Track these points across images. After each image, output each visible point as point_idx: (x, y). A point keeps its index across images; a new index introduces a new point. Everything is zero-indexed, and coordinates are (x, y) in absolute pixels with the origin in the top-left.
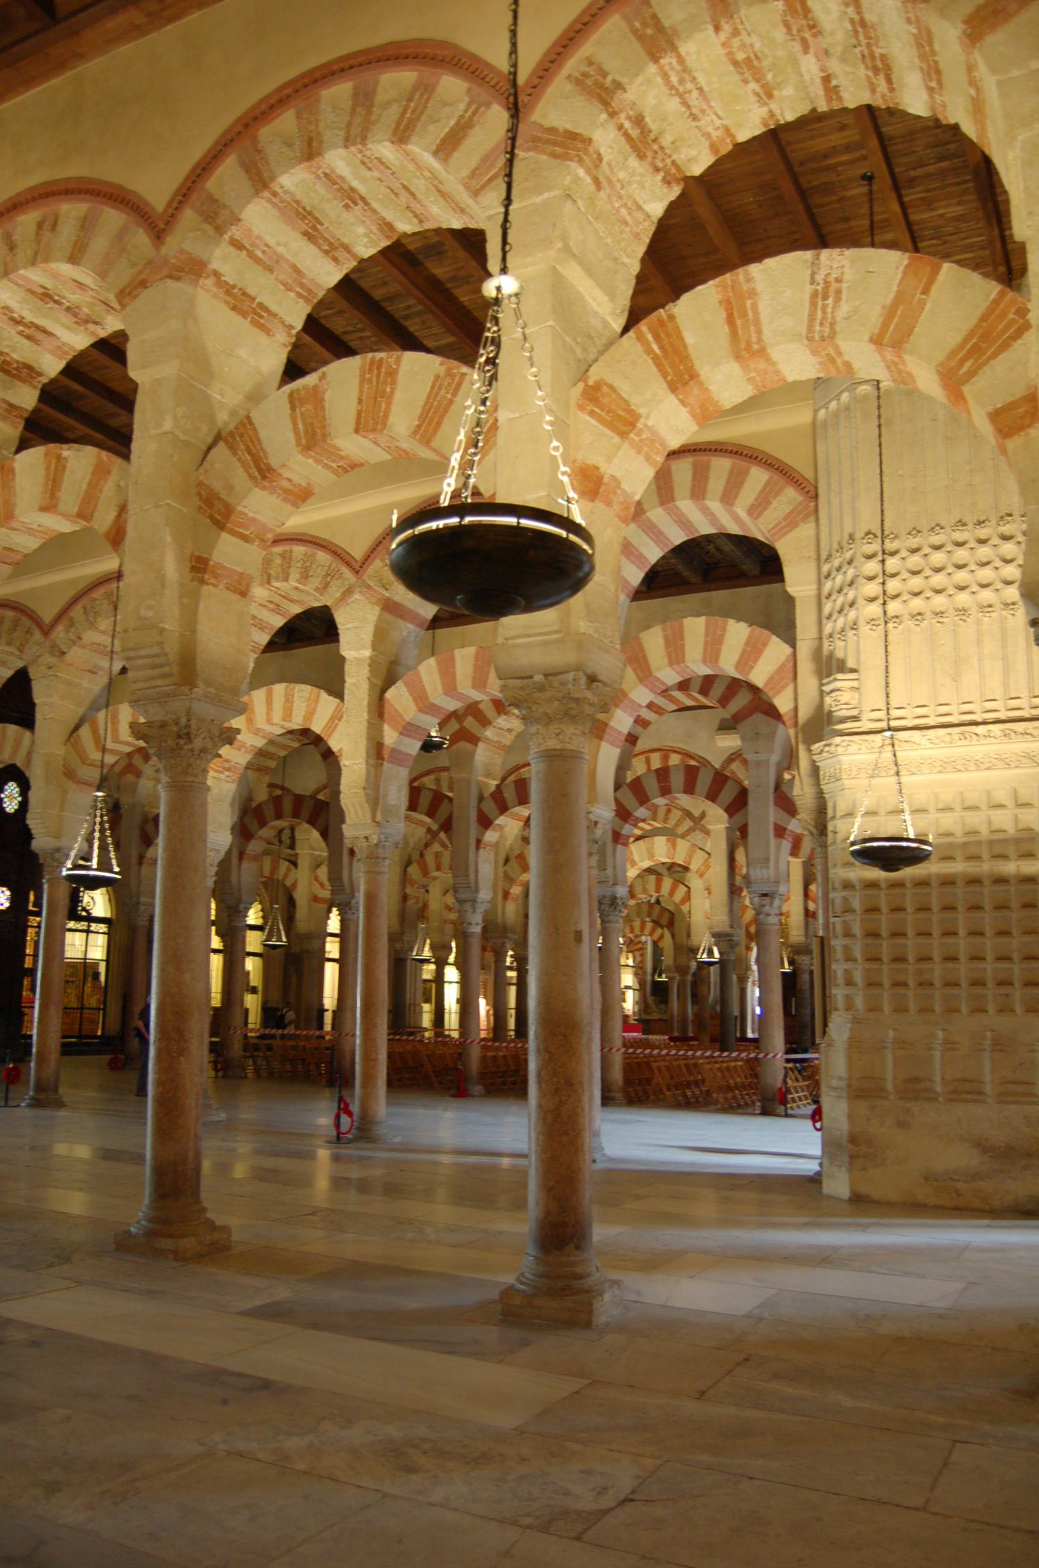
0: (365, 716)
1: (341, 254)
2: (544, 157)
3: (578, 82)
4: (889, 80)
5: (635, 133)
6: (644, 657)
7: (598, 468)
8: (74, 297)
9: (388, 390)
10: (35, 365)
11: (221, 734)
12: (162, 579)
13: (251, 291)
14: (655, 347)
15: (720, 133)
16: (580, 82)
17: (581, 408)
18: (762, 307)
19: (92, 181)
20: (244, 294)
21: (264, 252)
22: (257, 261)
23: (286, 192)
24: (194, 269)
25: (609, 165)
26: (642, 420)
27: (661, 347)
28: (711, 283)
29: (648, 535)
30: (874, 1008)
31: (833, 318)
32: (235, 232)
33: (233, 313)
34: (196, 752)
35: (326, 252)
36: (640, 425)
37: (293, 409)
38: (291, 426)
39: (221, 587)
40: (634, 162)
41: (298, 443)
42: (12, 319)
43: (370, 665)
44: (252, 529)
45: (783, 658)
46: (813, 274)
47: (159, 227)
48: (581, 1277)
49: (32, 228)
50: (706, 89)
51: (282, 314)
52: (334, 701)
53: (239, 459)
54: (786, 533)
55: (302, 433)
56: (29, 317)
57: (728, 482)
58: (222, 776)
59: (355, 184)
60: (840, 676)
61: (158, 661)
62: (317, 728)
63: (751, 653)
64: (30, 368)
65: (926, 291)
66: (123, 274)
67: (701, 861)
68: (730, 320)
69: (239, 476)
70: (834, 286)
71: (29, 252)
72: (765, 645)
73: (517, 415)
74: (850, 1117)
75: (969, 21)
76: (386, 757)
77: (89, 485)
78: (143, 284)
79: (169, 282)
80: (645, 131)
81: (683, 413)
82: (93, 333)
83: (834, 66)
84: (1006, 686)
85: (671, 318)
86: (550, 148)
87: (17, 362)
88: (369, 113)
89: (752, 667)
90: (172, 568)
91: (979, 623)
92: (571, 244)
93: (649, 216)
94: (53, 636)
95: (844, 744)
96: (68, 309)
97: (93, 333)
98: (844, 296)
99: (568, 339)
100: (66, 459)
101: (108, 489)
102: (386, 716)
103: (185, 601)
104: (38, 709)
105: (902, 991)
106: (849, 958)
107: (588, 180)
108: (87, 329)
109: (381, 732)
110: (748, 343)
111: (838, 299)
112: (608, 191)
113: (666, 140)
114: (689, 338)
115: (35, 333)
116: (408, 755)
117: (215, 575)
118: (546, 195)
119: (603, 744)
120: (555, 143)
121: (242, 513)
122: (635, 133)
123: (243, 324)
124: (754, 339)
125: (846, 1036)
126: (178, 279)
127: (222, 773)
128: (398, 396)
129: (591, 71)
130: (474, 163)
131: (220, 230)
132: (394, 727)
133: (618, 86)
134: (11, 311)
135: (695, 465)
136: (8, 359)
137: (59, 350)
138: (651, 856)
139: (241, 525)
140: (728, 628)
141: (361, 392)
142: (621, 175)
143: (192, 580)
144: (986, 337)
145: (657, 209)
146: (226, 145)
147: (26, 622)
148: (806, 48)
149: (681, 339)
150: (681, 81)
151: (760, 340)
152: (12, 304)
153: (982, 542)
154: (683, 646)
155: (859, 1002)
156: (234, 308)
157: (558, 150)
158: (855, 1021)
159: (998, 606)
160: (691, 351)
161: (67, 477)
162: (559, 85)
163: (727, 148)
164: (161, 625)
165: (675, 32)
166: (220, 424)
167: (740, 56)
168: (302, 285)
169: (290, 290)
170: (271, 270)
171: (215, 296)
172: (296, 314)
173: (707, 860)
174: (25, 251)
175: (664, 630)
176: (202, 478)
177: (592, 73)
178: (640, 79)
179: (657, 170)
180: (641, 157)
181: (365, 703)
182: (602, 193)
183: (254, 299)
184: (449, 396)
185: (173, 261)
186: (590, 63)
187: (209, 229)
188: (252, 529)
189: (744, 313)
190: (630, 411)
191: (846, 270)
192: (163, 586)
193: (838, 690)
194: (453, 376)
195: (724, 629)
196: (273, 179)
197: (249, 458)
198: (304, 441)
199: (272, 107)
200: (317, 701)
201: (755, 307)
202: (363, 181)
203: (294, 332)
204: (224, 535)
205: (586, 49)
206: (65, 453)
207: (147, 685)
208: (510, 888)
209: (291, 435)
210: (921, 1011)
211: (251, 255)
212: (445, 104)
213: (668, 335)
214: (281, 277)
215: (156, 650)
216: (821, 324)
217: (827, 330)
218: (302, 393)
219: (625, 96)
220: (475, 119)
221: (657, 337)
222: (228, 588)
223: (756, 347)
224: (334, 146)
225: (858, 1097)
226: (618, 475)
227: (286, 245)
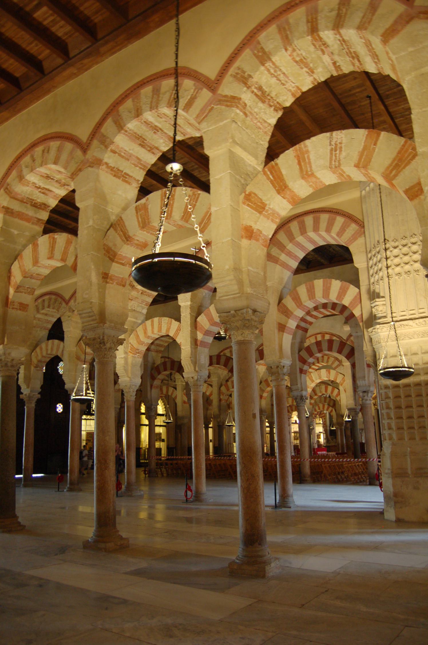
0: (189, 328)
1: (155, 151)
2: (223, 107)
3: (235, 77)
4: (359, 61)
5: (259, 93)
6: (299, 297)
7: (251, 227)
8: (58, 177)
9: (172, 202)
10: (46, 203)
11: (118, 341)
12: (91, 283)
13: (121, 169)
14: (271, 177)
15: (295, 89)
17: (244, 203)
18: (312, 157)
19: (60, 133)
20: (118, 170)
21: (124, 153)
22: (122, 157)
23: (130, 130)
24: (98, 162)
25: (250, 106)
26: (268, 206)
27: (273, 177)
28: (291, 149)
29: (297, 247)
30: (401, 439)
31: (339, 158)
32: (112, 147)
33: (114, 178)
34: (108, 349)
35: (149, 151)
36: (267, 208)
37: (137, 213)
38: (136, 220)
39: (115, 284)
40: (260, 105)
41: (139, 226)
42: (36, 187)
43: (190, 308)
44: (125, 260)
45: (355, 294)
46: (331, 141)
47: (84, 148)
48: (261, 557)
49: (41, 152)
50: (286, 73)
51: (134, 176)
52: (177, 323)
53: (118, 234)
54: (353, 242)
55: (141, 222)
56: (42, 186)
57: (328, 224)
58: (136, 356)
59: (157, 124)
60: (377, 300)
61: (91, 314)
62: (171, 334)
63: (342, 293)
64: (45, 204)
65: (375, 144)
66: (73, 167)
67: (341, 379)
68: (299, 163)
69: (118, 241)
70: (339, 145)
71: (40, 162)
72: (348, 289)
73: (218, 209)
74: (394, 486)
75: (383, 35)
76: (199, 344)
77: (65, 248)
78: (80, 170)
79: (90, 169)
80: (263, 92)
81: (285, 201)
82: (67, 189)
83: (336, 58)
85: (277, 164)
86: (225, 103)
87: (40, 203)
88: (159, 97)
89: (343, 298)
90: (94, 278)
92: (236, 139)
93: (270, 124)
94: (70, 304)
95: (381, 328)
96: (57, 181)
97: (67, 189)
98: (343, 149)
99: (238, 177)
100: (56, 238)
101: (72, 249)
102: (198, 328)
103: (100, 290)
104: (65, 333)
105: (412, 431)
106: (389, 418)
107: (241, 114)
108: (64, 188)
109: (196, 334)
110: (307, 172)
111: (341, 151)
112: (251, 117)
113: (273, 94)
114: (284, 172)
115: (45, 191)
116: (207, 343)
117: (111, 279)
118: (225, 122)
119: (285, 334)
120: (227, 101)
121: (120, 255)
122: (259, 93)
123: (119, 181)
124: (309, 170)
125: (390, 450)
126: (92, 167)
127: (136, 354)
129: (239, 72)
130: (197, 112)
131: (106, 147)
132: (201, 332)
133: (250, 76)
134: (36, 184)
135: (314, 218)
136: (36, 202)
137: (55, 196)
138: (320, 378)
139: (120, 259)
140: (332, 283)
142: (256, 110)
143: (103, 282)
144: (400, 160)
145: (273, 121)
146: (107, 115)
147: (60, 300)
148: (323, 52)
149: (281, 172)
150: (275, 71)
151: (311, 170)
152: (36, 181)
154: (314, 291)
155: (395, 436)
156: (115, 176)
158: (393, 444)
160: (285, 177)
161: (57, 246)
162: (228, 79)
163: (299, 94)
164: (91, 300)
165: (270, 53)
166: (112, 220)
167: (298, 59)
168: (141, 164)
169: (137, 166)
170: (128, 160)
171: (107, 172)
172: (140, 175)
173: (343, 378)
174: (38, 161)
175: (306, 286)
176: (105, 242)
177: (240, 72)
178: (258, 73)
179: (271, 106)
180: (263, 102)
181: (189, 323)
182: (248, 118)
183: (123, 171)
184: (194, 203)
185: (90, 160)
186: (239, 68)
187: (102, 146)
188: (125, 260)
189: (304, 160)
190: (263, 203)
191: (343, 139)
192: (91, 284)
193: (377, 306)
194: (195, 195)
195: (330, 284)
196: (125, 126)
197: (121, 233)
198: (141, 225)
199: (123, 99)
200: (171, 324)
201: (308, 157)
202: (160, 123)
203: (140, 182)
204: (114, 264)
205: (237, 64)
206: (56, 237)
207: (87, 324)
208: (263, 394)
209: (137, 223)
210: (421, 439)
211: (120, 155)
212: (186, 91)
213: (275, 172)
214: (133, 162)
215: (89, 310)
216: (335, 161)
217: (337, 163)
218: (140, 206)
219: (253, 80)
220: (197, 95)
221: (271, 173)
222: (117, 284)
223: (310, 173)
224: (147, 111)
225: (396, 477)
226: (260, 229)
227: (133, 150)
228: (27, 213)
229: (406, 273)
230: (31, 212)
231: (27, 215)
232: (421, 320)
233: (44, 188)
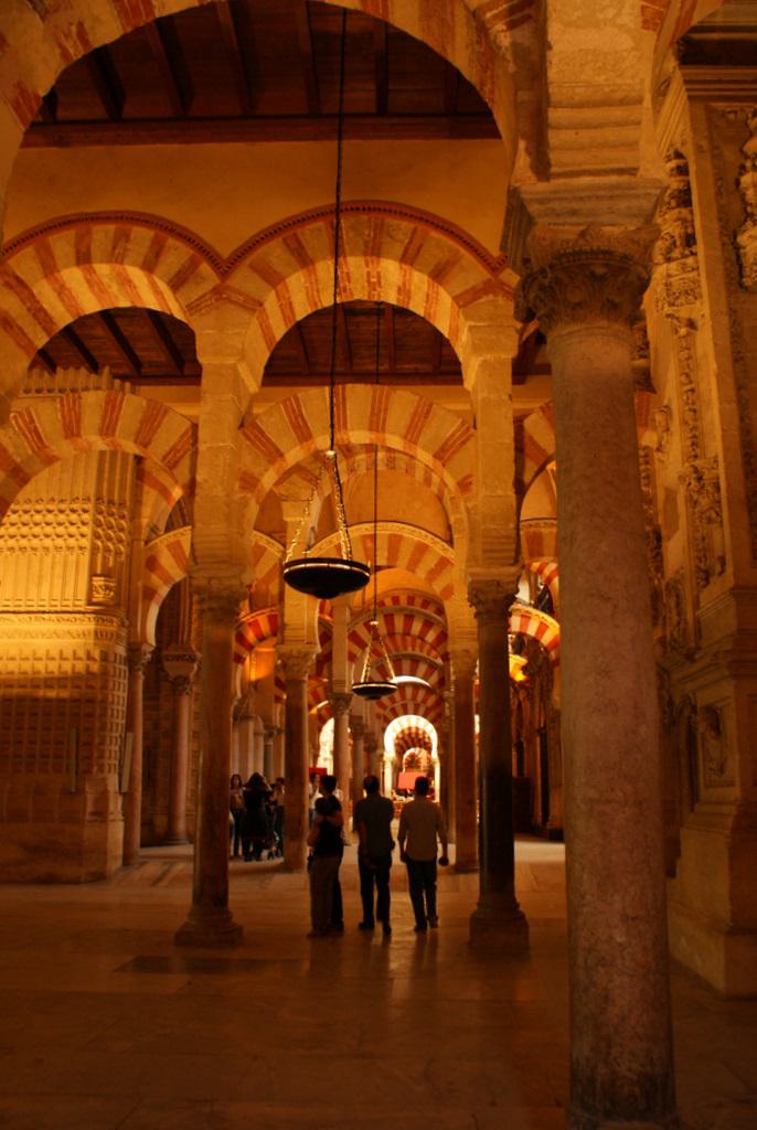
84: (63, 593)
91: (54, 557)
153: (61, 511)
159: (64, 548)
229: (20, 549)
232: (26, 616)
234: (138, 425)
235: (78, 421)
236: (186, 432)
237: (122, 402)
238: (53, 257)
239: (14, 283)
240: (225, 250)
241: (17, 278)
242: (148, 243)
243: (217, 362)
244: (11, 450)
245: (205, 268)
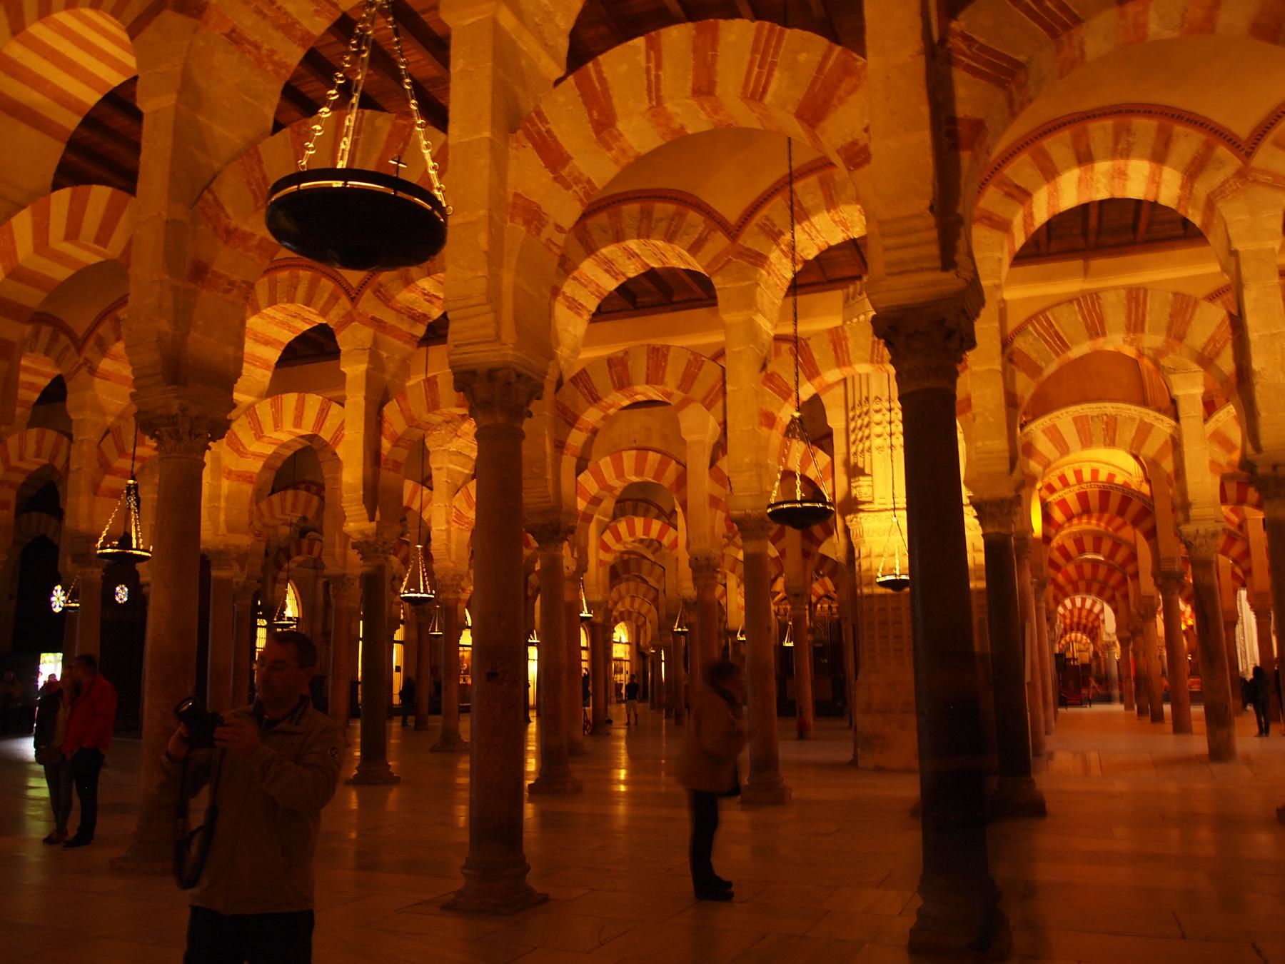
16: (762, 227)
56: (432, 292)
114: (816, 356)
120: (751, 257)
128: (669, 368)
141: (648, 363)
157: (752, 260)
162: (752, 227)
192: (545, 456)
205: (765, 211)
212: (692, 226)
228: (400, 327)
230: (405, 326)
231: (401, 330)
233: (434, 296)
234: (1167, 318)
235: (1102, 322)
236: (1223, 321)
237: (1145, 299)
238: (1051, 161)
239: (1015, 192)
240: (1242, 130)
241: (1017, 187)
242: (1152, 134)
243: (1252, 246)
244: (1034, 356)
245: (1222, 151)
